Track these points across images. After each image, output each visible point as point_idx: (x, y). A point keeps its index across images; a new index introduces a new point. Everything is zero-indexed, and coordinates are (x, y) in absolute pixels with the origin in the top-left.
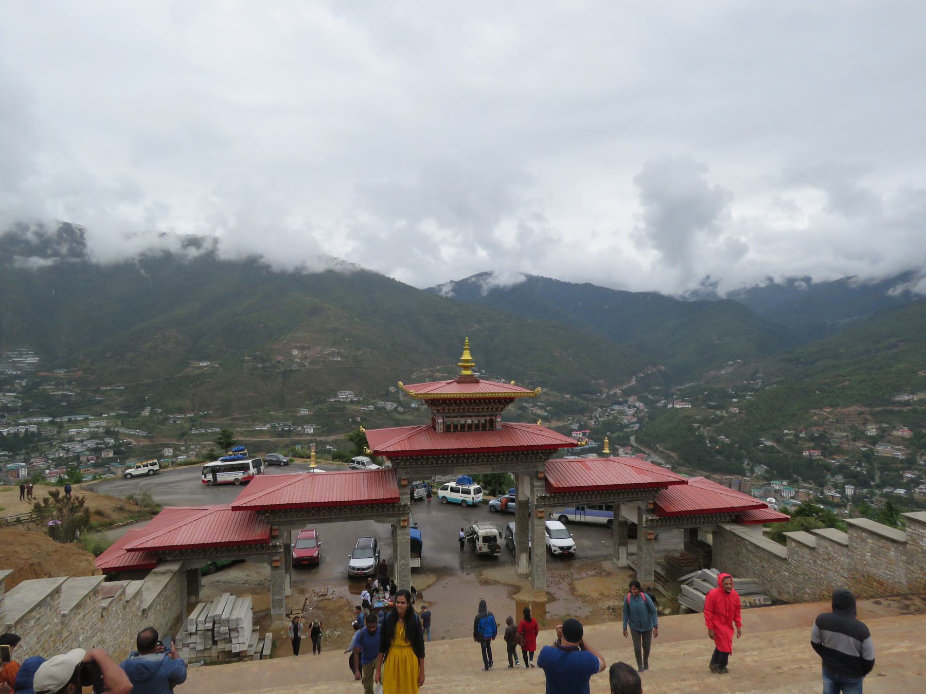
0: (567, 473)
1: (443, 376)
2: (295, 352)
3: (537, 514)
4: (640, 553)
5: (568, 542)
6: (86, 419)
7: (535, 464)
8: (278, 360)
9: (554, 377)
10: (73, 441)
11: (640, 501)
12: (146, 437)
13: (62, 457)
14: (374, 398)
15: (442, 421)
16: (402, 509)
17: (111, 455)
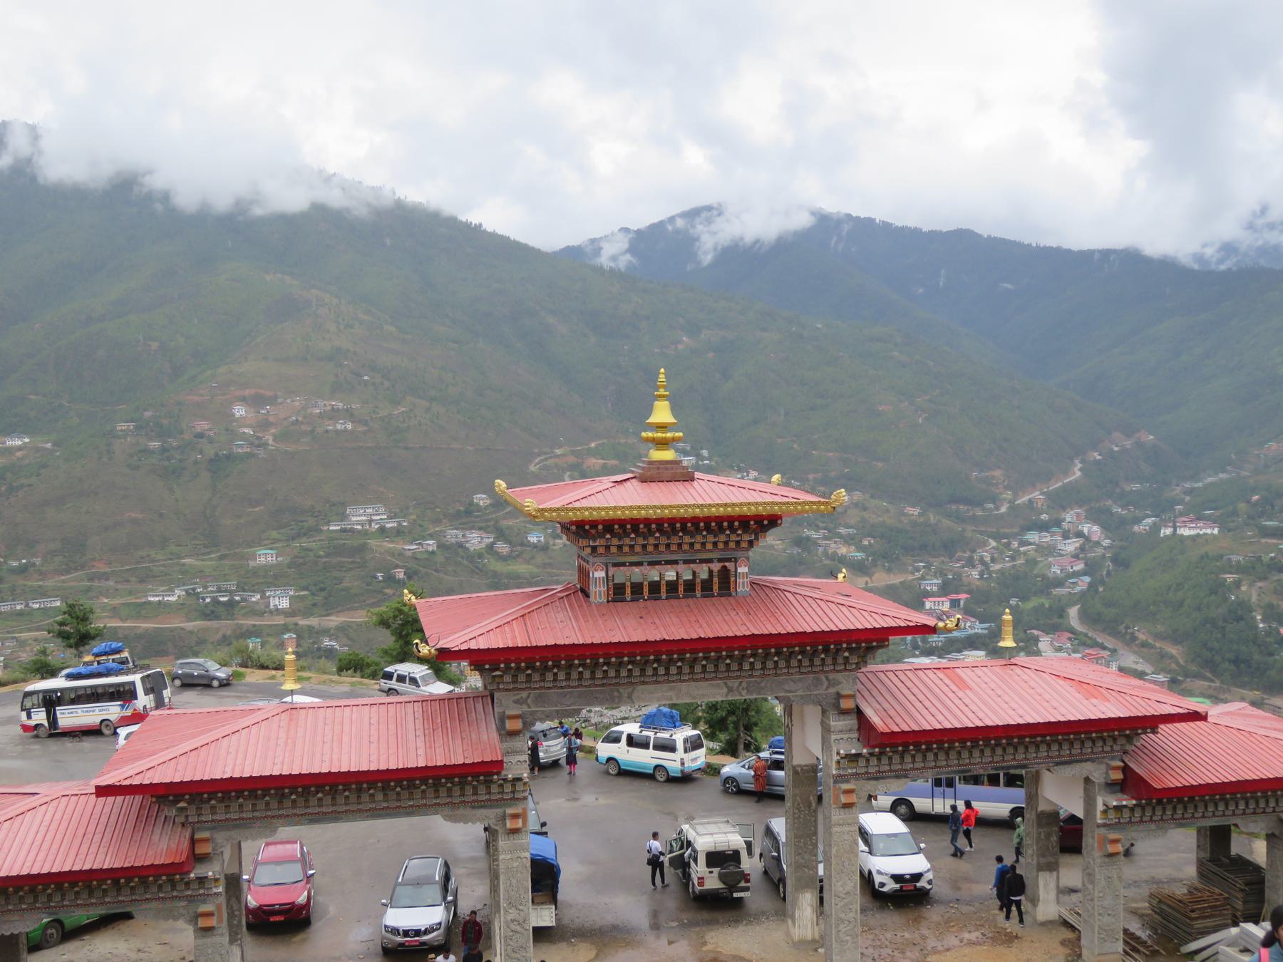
0: (912, 698)
1: (605, 463)
2: (239, 411)
3: (837, 798)
4: (1090, 887)
5: (914, 863)
7: (831, 676)
8: (199, 430)
9: (880, 464)
11: (1088, 763)
14: (437, 521)
15: (602, 574)
16: (508, 788)
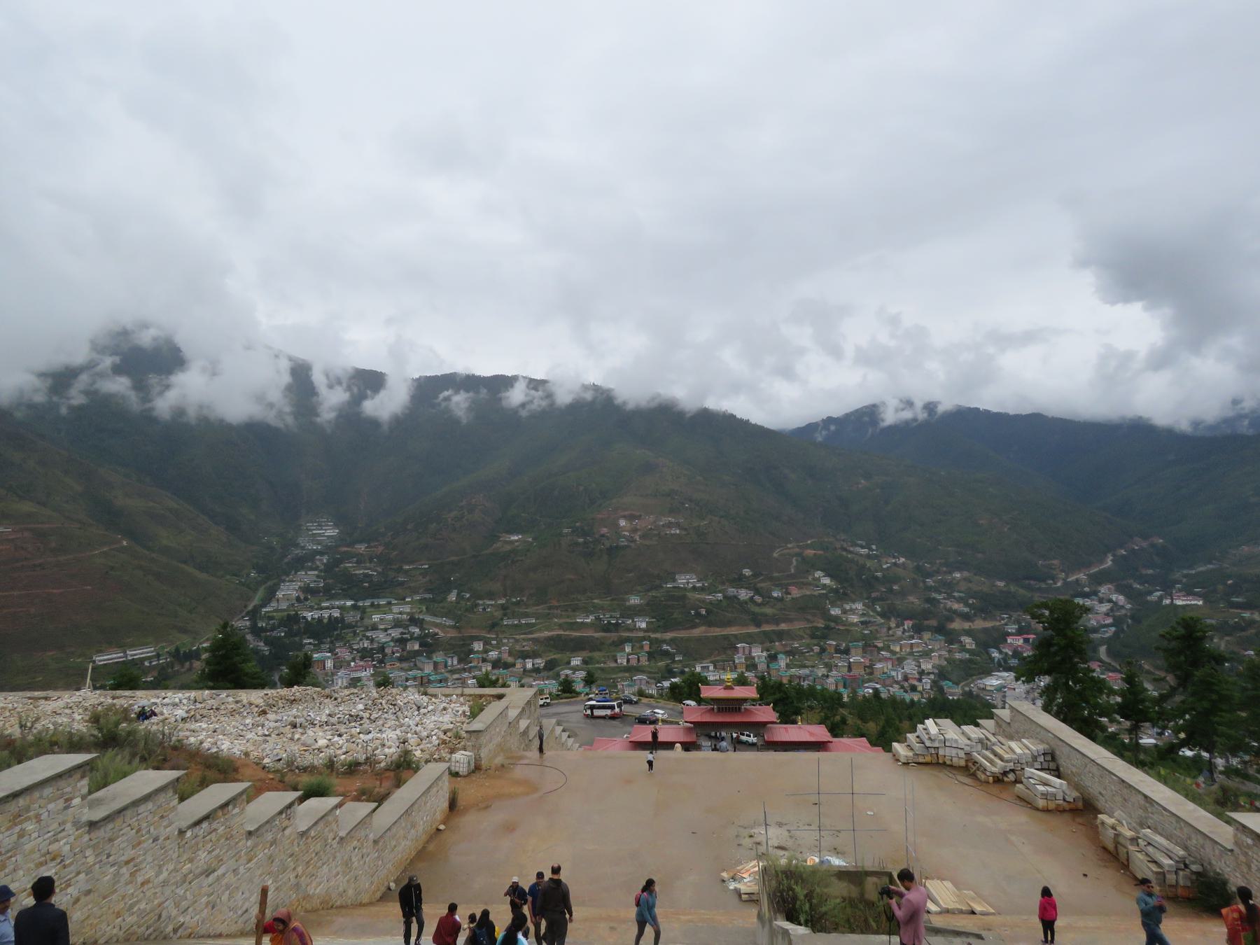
1: (815, 553)
2: (623, 523)
6: (389, 603)
8: (602, 532)
10: (377, 629)
12: (454, 627)
13: (367, 648)
14: (723, 583)
17: (417, 647)
